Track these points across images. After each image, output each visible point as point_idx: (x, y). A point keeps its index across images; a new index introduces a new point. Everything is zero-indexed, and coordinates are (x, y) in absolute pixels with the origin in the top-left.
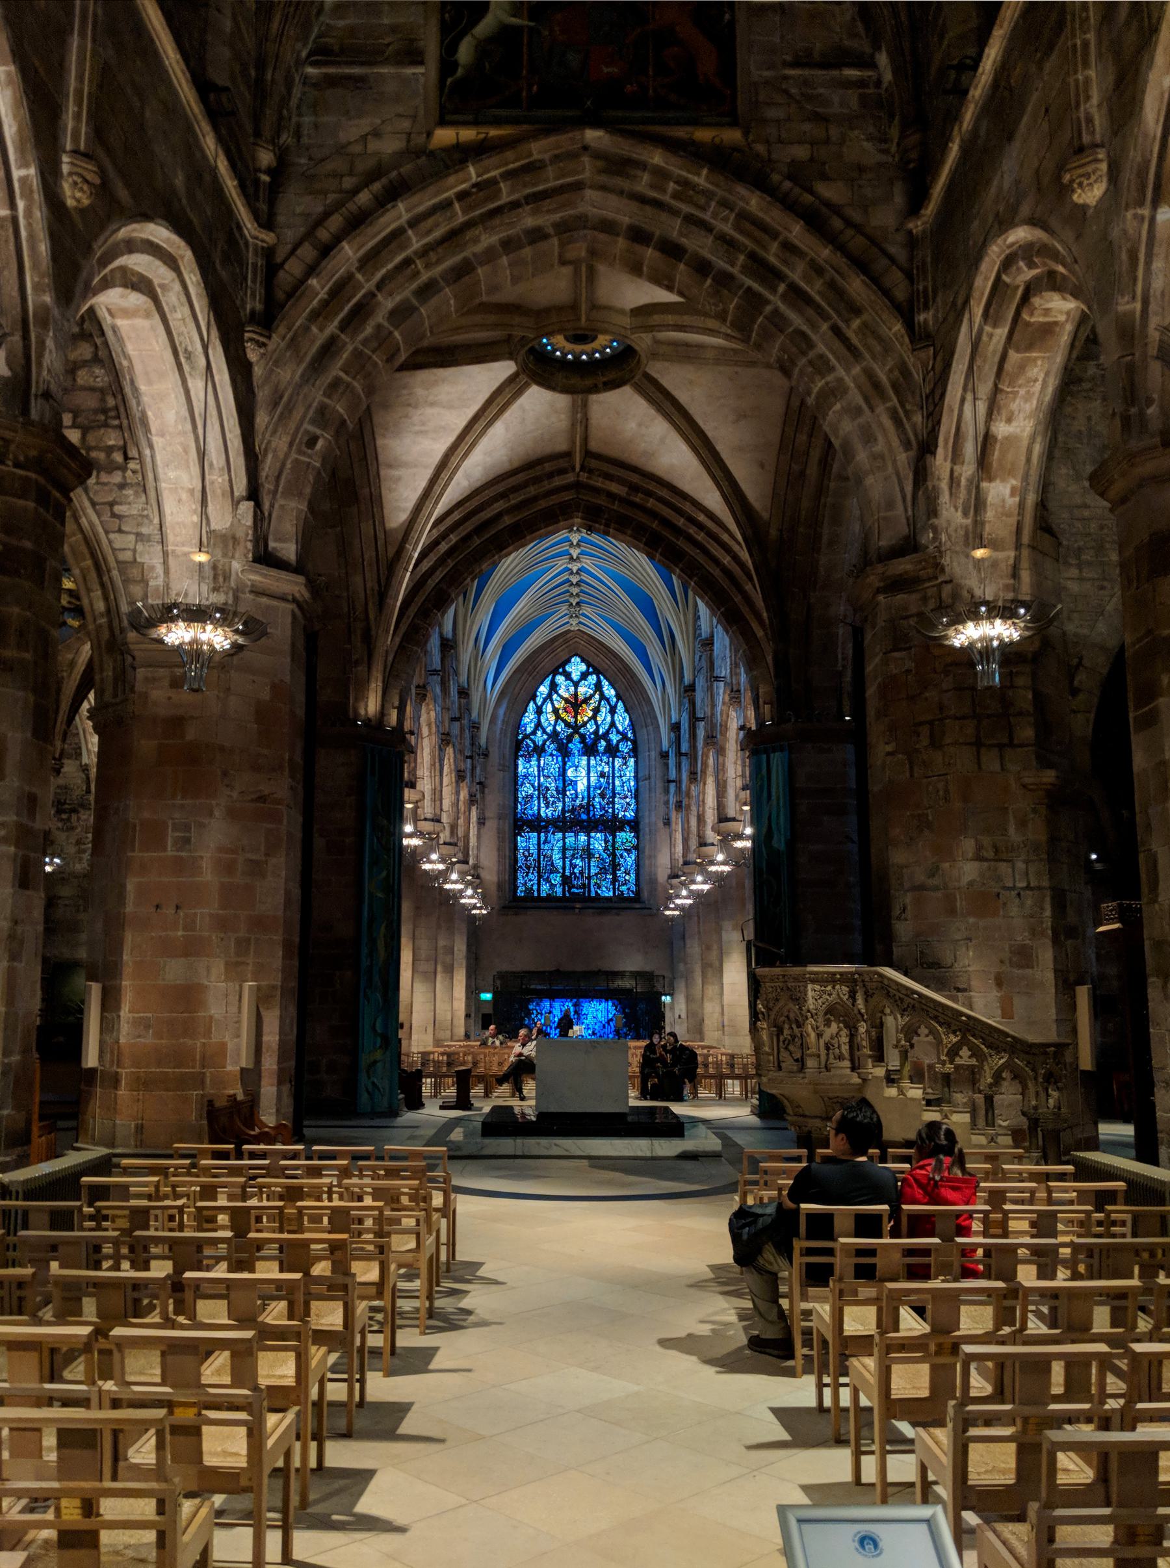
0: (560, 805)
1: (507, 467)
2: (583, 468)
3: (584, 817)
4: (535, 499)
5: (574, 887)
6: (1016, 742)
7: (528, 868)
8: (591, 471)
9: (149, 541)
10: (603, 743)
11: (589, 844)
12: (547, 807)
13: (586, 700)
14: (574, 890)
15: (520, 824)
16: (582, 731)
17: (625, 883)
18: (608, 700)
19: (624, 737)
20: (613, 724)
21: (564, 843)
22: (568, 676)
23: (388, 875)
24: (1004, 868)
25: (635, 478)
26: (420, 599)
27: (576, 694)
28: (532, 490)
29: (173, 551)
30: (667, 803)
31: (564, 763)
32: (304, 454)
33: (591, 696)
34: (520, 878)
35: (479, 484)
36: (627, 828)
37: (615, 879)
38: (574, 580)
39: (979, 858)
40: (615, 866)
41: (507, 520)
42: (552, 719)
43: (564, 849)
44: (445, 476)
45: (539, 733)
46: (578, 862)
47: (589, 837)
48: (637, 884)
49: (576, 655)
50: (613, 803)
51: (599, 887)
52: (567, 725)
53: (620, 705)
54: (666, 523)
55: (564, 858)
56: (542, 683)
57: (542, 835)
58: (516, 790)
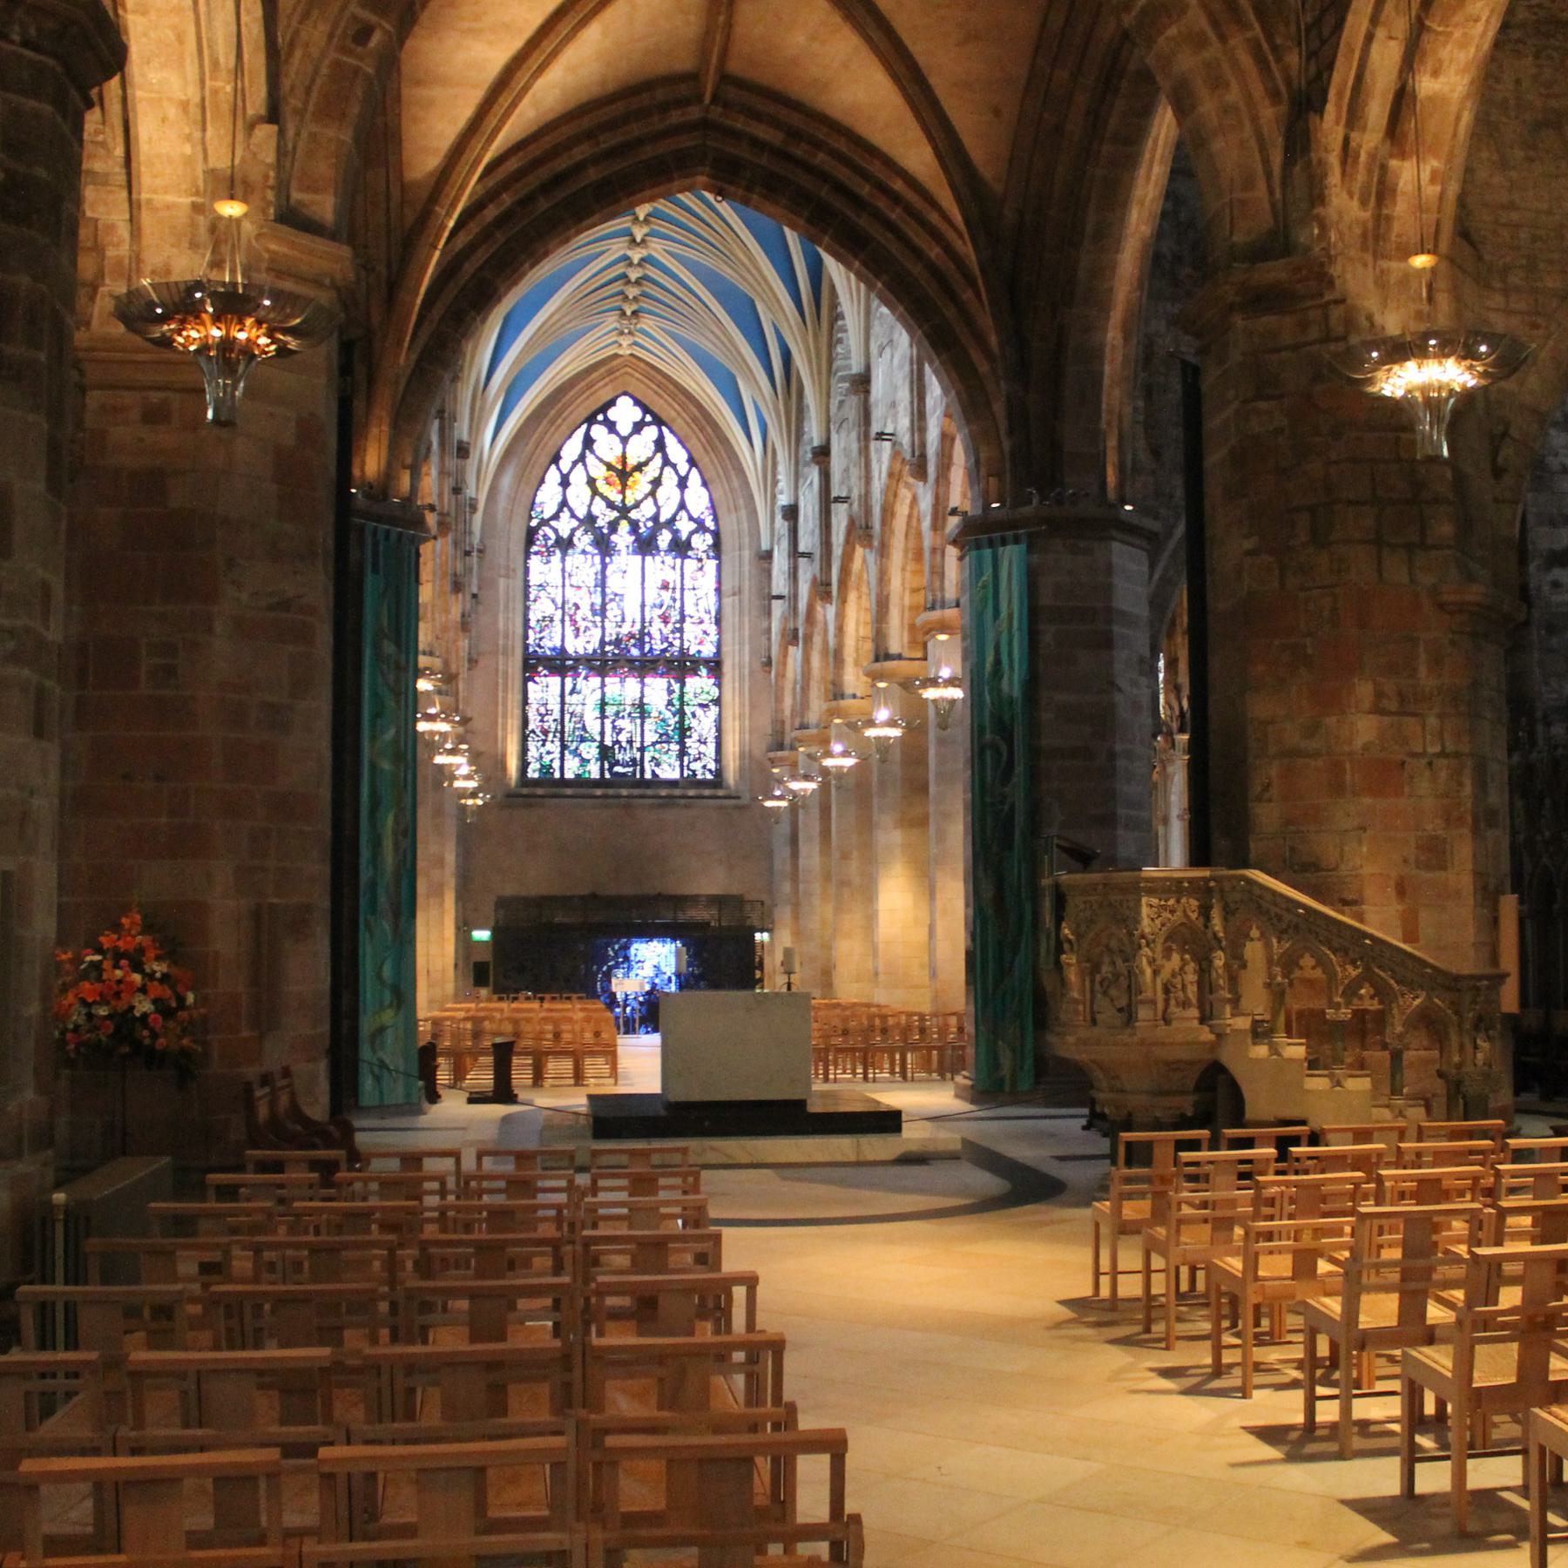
0: (597, 633)
1: (596, 91)
2: (715, 99)
3: (635, 652)
4: (639, 142)
5: (617, 763)
6: (1429, 541)
7: (546, 733)
8: (726, 105)
9: (106, 184)
12: (577, 636)
13: (639, 467)
14: (618, 769)
15: (533, 664)
16: (633, 515)
18: (674, 466)
19: (701, 527)
20: (682, 506)
21: (603, 694)
22: (611, 426)
23: (398, 732)
24: (1411, 724)
25: (796, 120)
26: (452, 291)
27: (624, 458)
28: (635, 130)
29: (149, 201)
30: (769, 630)
31: (604, 566)
32: (350, 53)
33: (650, 460)
34: (532, 746)
35: (551, 116)
36: (704, 671)
37: (682, 753)
38: (634, 275)
39: (1378, 710)
40: (683, 731)
41: (593, 174)
42: (588, 492)
43: (603, 704)
44: (505, 101)
45: (565, 515)
46: (623, 723)
47: (642, 683)
48: (718, 760)
49: (625, 393)
50: (681, 630)
53: (695, 478)
54: (841, 189)
55: (603, 717)
58: (527, 609)
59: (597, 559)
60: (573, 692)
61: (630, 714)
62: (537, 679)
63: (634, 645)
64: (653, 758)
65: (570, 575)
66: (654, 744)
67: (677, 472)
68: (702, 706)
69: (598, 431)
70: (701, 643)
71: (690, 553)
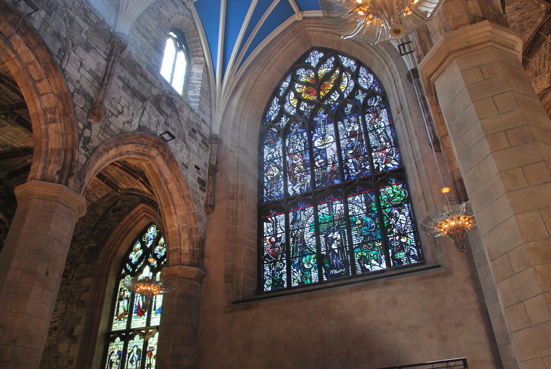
0: (308, 178)
3: (337, 182)
5: (332, 267)
7: (275, 255)
10: (350, 106)
11: (347, 210)
17: (402, 247)
18: (348, 69)
20: (357, 87)
21: (316, 217)
22: (308, 67)
31: (310, 136)
34: (267, 269)
40: (384, 230)
42: (295, 103)
43: (317, 224)
45: (283, 119)
47: (346, 203)
49: (313, 49)
50: (371, 159)
51: (367, 262)
52: (309, 102)
53: (362, 71)
55: (317, 234)
56: (284, 79)
57: (291, 214)
59: (305, 134)
60: (294, 221)
61: (338, 227)
62: (269, 219)
63: (337, 178)
64: (362, 256)
65: (288, 149)
66: (360, 246)
67: (351, 72)
68: (395, 206)
69: (301, 72)
70: (387, 162)
71: (368, 110)
